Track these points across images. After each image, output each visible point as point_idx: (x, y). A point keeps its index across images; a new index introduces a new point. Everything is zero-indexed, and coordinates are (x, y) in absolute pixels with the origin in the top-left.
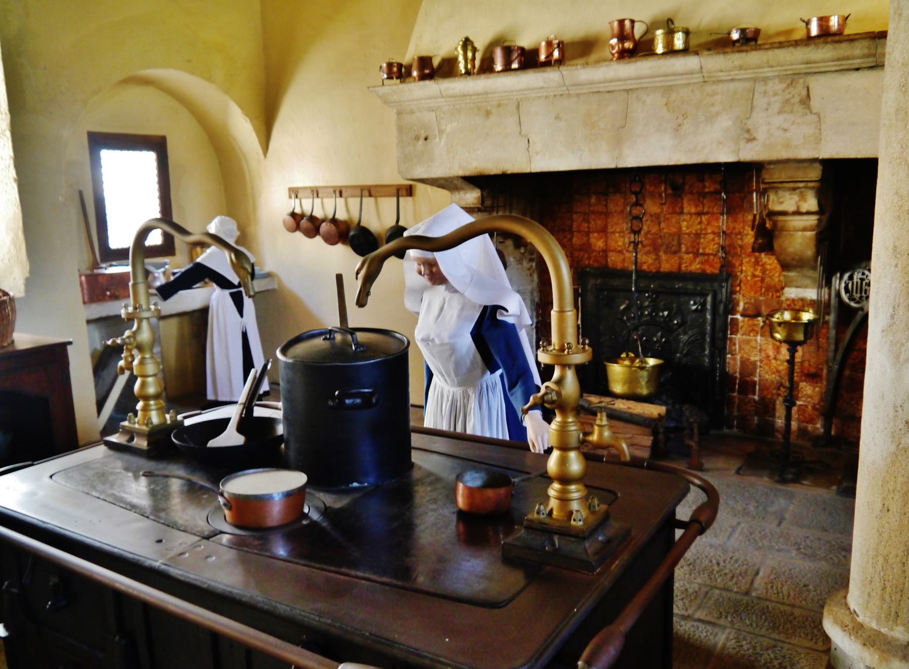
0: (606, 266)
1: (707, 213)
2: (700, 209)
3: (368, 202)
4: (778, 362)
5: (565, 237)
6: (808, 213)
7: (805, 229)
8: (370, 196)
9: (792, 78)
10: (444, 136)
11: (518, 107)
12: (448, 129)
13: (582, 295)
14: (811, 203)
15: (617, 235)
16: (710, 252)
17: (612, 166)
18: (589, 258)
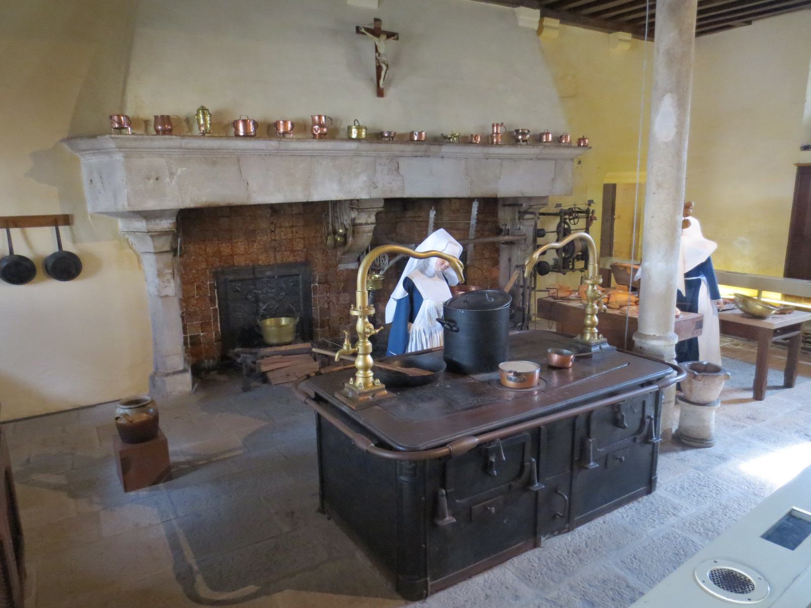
0: (234, 265)
1: (296, 226)
2: (291, 224)
3: (15, 232)
4: (339, 306)
5: (200, 248)
6: (372, 224)
7: (369, 232)
8: (16, 226)
9: (394, 158)
10: (175, 177)
11: (238, 160)
12: (179, 171)
13: (218, 288)
14: (373, 219)
15: (239, 243)
16: (299, 249)
17: (305, 200)
18: (220, 261)
